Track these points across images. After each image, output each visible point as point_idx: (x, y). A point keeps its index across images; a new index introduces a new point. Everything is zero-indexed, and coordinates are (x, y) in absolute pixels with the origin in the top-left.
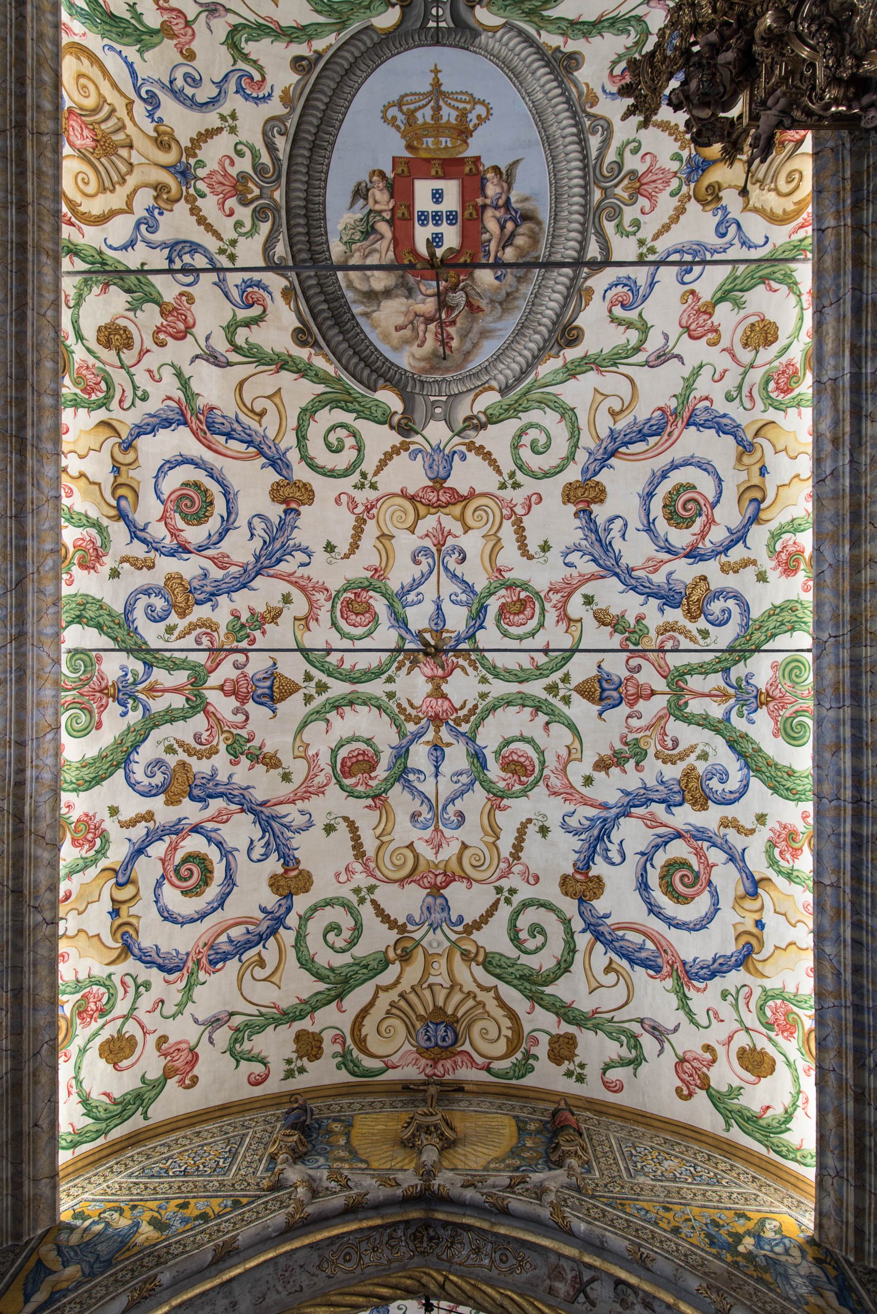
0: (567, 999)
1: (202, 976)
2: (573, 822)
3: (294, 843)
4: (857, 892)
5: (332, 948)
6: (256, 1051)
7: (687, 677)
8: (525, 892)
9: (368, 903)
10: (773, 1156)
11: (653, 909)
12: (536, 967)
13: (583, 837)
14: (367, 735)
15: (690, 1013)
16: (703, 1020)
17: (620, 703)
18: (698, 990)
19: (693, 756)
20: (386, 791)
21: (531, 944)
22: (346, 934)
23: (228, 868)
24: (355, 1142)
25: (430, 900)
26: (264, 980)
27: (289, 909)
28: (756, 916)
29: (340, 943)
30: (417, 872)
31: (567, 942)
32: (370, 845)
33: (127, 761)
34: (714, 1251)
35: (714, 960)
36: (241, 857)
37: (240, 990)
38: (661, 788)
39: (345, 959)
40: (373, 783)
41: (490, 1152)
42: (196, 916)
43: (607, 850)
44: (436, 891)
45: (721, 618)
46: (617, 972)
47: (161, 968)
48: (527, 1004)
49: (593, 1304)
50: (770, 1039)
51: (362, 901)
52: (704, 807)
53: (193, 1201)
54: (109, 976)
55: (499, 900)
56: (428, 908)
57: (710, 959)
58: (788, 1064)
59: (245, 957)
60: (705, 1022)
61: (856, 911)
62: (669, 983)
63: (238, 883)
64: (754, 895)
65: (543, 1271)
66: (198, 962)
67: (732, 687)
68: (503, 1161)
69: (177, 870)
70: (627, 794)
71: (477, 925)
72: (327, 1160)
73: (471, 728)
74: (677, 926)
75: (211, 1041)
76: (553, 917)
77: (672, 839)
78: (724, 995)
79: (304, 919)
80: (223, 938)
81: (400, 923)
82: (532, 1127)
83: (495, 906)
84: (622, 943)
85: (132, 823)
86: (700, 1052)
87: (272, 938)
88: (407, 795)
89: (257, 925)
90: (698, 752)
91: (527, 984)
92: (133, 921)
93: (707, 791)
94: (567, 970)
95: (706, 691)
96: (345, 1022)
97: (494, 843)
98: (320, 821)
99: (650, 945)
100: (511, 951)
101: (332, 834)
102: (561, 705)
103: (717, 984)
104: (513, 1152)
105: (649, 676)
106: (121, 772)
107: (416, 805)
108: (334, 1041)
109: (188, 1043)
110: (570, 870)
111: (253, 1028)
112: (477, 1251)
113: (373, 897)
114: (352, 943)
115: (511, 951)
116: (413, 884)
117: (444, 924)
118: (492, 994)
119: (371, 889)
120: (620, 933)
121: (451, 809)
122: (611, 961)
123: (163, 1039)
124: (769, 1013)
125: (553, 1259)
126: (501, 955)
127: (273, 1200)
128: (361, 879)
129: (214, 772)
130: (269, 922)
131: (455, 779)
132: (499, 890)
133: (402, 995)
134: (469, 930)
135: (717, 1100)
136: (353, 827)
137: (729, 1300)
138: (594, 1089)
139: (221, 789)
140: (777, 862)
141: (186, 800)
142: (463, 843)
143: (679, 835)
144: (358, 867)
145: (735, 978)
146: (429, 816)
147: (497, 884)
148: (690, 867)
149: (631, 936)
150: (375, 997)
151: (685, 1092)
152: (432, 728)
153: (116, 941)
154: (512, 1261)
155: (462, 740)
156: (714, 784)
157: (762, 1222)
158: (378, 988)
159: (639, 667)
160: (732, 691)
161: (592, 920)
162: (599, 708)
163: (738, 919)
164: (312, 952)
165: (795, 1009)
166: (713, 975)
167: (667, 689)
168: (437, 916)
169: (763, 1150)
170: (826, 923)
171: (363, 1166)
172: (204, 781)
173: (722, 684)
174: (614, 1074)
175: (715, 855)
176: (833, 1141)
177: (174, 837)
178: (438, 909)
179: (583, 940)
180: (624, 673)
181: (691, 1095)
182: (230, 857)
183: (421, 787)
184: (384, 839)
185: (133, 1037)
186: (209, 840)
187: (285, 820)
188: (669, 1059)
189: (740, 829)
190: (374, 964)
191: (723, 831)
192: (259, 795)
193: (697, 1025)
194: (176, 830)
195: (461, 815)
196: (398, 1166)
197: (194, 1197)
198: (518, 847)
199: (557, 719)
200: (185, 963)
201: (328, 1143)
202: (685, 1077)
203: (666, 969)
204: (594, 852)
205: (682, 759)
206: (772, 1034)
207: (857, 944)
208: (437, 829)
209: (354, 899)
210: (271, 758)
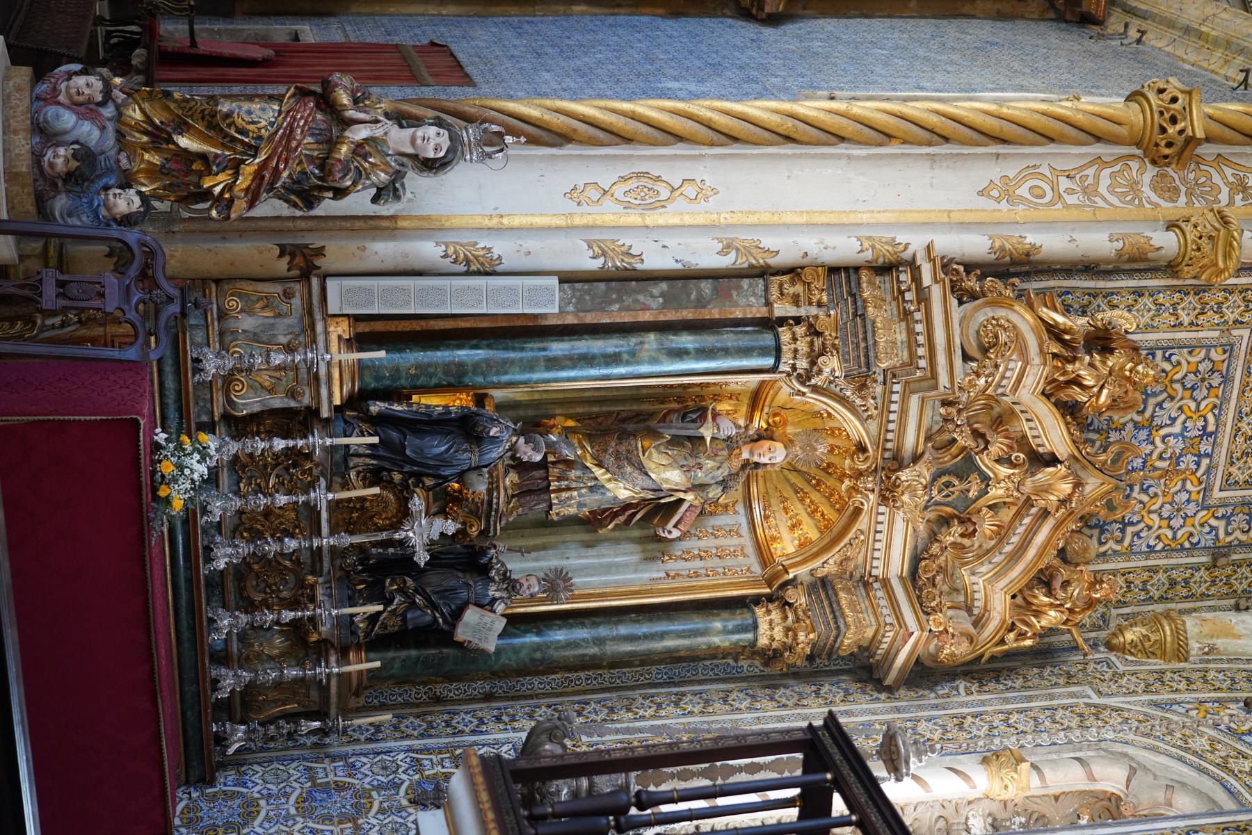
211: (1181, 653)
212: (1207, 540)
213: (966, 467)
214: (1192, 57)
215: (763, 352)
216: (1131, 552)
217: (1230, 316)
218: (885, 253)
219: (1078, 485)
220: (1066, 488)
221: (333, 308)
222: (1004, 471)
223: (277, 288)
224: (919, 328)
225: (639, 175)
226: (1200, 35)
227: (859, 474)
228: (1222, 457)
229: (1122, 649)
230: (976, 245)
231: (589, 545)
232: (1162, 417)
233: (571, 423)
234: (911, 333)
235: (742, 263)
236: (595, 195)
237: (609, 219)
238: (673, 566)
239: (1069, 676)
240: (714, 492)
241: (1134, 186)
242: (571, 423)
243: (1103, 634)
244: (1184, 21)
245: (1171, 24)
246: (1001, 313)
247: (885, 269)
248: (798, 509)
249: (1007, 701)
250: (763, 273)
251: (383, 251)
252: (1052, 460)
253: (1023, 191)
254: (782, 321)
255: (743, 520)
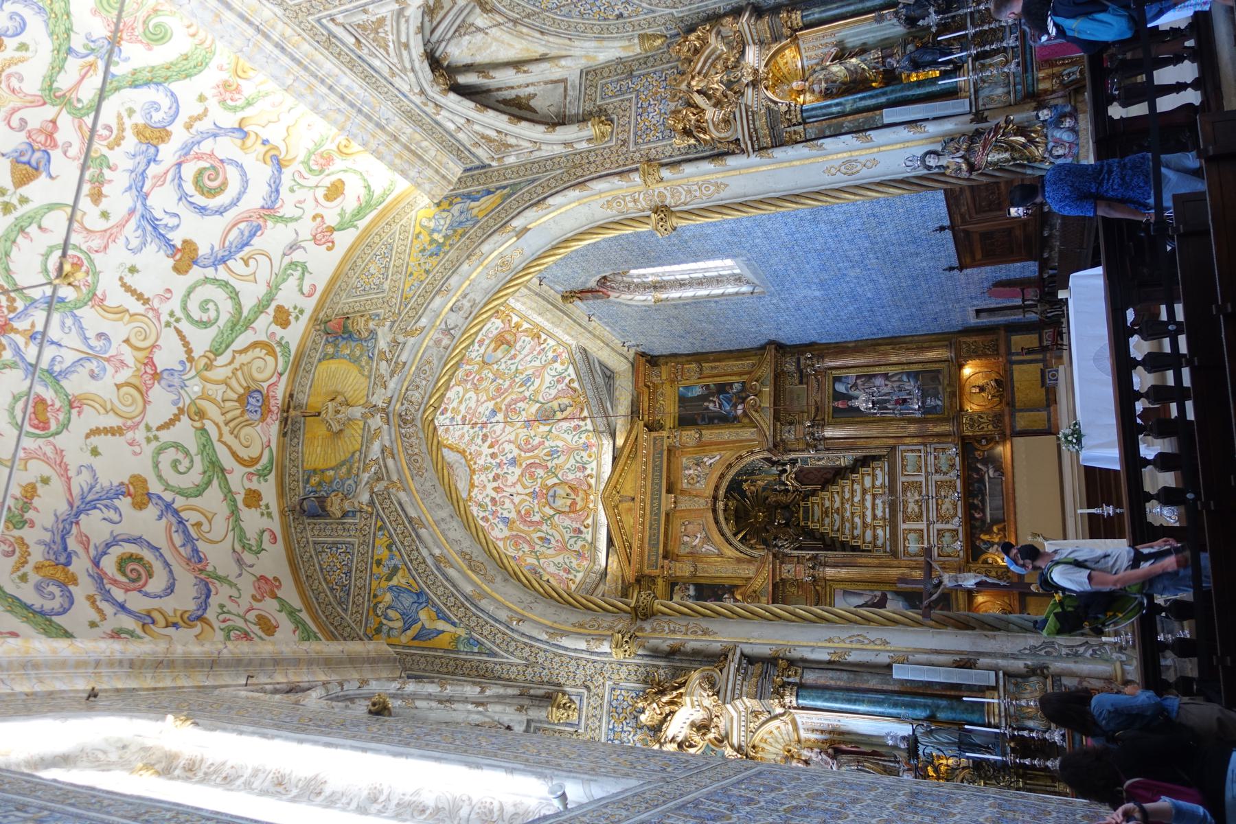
0: (255, 301)
1: (210, 568)
2: (135, 243)
3: (106, 484)
4: (306, 68)
5: (189, 469)
6: (256, 537)
7: (55, 85)
8: (175, 304)
9: (159, 434)
10: (380, 208)
11: (220, 211)
12: (228, 316)
13: (149, 240)
14: (9, 399)
15: (292, 219)
16: (298, 213)
17: (48, 154)
18: (282, 206)
19: (126, 120)
20: (67, 395)
21: (213, 314)
22: (180, 456)
23: (127, 541)
24: (333, 464)
25: (163, 382)
26: (210, 523)
27: (160, 498)
28: (260, 141)
29: (186, 463)
30: (140, 387)
31: (220, 286)
32: (112, 421)
33: (42, 613)
34: (442, 255)
35: (270, 186)
36: (118, 529)
37: (217, 542)
38: (138, 159)
39: (197, 459)
40: (58, 405)
41: (353, 375)
42: (168, 569)
43: (166, 226)
44: (157, 376)
45: (17, 24)
46: (250, 258)
47: (208, 596)
48: (250, 332)
49: (457, 326)
50: (328, 175)
51: (156, 438)
52: (169, 134)
53: (375, 558)
54: (222, 630)
55: (175, 328)
56: (170, 386)
57: (268, 188)
58: (345, 171)
59: (195, 536)
60: (301, 211)
61: (316, 77)
62: (270, 224)
63: (139, 535)
64: (246, 134)
65: (435, 351)
66: (201, 570)
67: (87, 55)
68: (362, 367)
69: (134, 581)
70: (130, 188)
71: (189, 351)
72: (348, 479)
73: (22, 299)
74: (238, 199)
75: (251, 566)
76: (199, 289)
77: (180, 172)
78: (292, 190)
79: (168, 487)
80: (182, 550)
81: (177, 412)
82: (330, 350)
83: (179, 332)
84: (234, 245)
85: (100, 611)
86: (314, 224)
87: (181, 514)
88: (73, 377)
89: (171, 524)
90: (125, 114)
91: (238, 327)
92: (179, 614)
93: (159, 125)
94: (237, 294)
95: (78, 77)
96: (240, 470)
97: (131, 316)
98: (87, 459)
99: (242, 226)
100: (212, 332)
101: (100, 450)
102: (26, 208)
103: (284, 190)
104: (355, 360)
105: (37, 117)
106: (55, 619)
107: (83, 372)
108: (250, 480)
109: (254, 583)
110: (171, 262)
111: (242, 537)
112: (418, 387)
113: (154, 429)
114: (187, 453)
115: (212, 332)
116: (149, 393)
117: (183, 377)
118: (237, 355)
119: (148, 429)
120: (227, 243)
121: (93, 342)
122: (242, 259)
123: (254, 597)
124: (315, 167)
125: (431, 343)
126: (214, 340)
127: (381, 504)
128: (140, 434)
129: (40, 542)
130: (170, 515)
131: (67, 330)
132: (168, 324)
133: (226, 424)
134: (191, 359)
135: (341, 228)
136: (96, 432)
137: (477, 251)
138: (309, 305)
139: (58, 539)
140: (236, 107)
141: (71, 568)
142: (124, 341)
143: (179, 165)
144: (130, 435)
145: (287, 175)
146: (95, 363)
147: (163, 324)
148: (205, 169)
149: (231, 237)
150: (225, 443)
151: (330, 244)
152: (12, 335)
153: (196, 625)
154: (427, 368)
155: (31, 311)
156: (157, 117)
157: (422, 226)
158: (219, 440)
159: (23, 122)
160: (91, 58)
161: (212, 260)
162: (44, 175)
163: (254, 155)
164: (191, 485)
165: (322, 149)
166: (277, 191)
167: (57, 108)
168: (176, 381)
169: (375, 213)
170: (310, 98)
171: (357, 454)
172: (51, 552)
173: (81, 61)
174: (306, 290)
175: (206, 147)
176: (406, 166)
177: (105, 581)
178: (171, 378)
179: (222, 273)
180: (21, 137)
181: (333, 242)
182: (118, 538)
183: (68, 363)
184: (109, 407)
185: (257, 616)
186: (105, 553)
187: (86, 489)
188: (310, 245)
189: (199, 118)
190: (203, 439)
191: (193, 131)
192: (63, 508)
193: (300, 218)
194: (99, 578)
195: (100, 335)
196: (360, 432)
197: (372, 558)
198: (140, 297)
199: (39, 217)
200: (202, 580)
201: (331, 482)
202: (323, 240)
203: (261, 222)
204: (164, 236)
205: (123, 130)
206: (327, 172)
207: (330, 88)
208: (108, 360)
209: (154, 444)
210: (26, 491)
211: (641, 37)
212: (634, 80)
213: (729, 85)
214: (606, 333)
215: (807, 110)
216: (662, 71)
217: (637, 154)
218: (763, 153)
219: (689, 83)
220: (694, 83)
221: (967, 101)
222: (716, 86)
223: (987, 107)
224: (751, 126)
225: (852, 174)
226: (603, 342)
227: (766, 79)
228: (634, 108)
229: (662, 36)
230: (731, 161)
231: (864, 44)
232: (657, 118)
233: (874, 84)
234: (754, 125)
235: (815, 142)
236: (869, 164)
237: (864, 152)
238: (833, 40)
239: (682, 21)
240: (818, 68)
241: (673, 196)
242: (874, 84)
243: (668, 41)
244: (609, 349)
245: (613, 349)
246: (722, 135)
247: (761, 149)
248: (785, 71)
249: (706, 6)
250: (807, 141)
251: (949, 126)
252: (699, 92)
253: (712, 188)
254: (800, 124)
255: (805, 64)
